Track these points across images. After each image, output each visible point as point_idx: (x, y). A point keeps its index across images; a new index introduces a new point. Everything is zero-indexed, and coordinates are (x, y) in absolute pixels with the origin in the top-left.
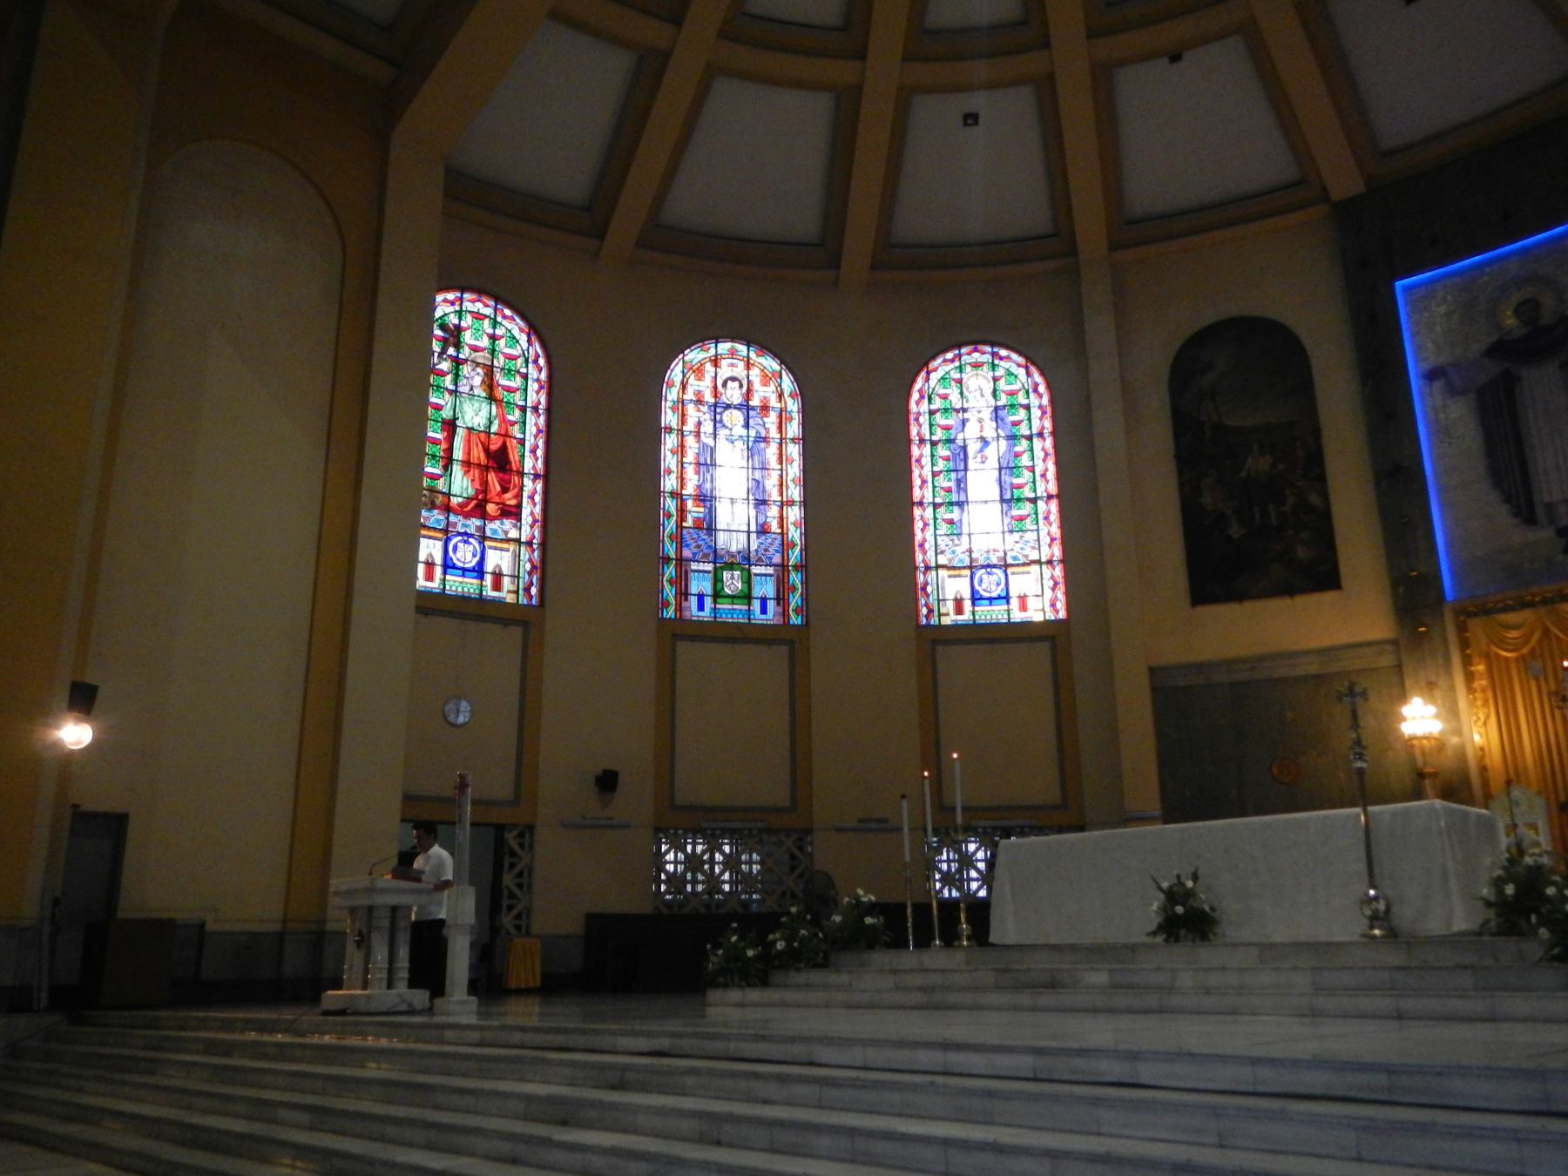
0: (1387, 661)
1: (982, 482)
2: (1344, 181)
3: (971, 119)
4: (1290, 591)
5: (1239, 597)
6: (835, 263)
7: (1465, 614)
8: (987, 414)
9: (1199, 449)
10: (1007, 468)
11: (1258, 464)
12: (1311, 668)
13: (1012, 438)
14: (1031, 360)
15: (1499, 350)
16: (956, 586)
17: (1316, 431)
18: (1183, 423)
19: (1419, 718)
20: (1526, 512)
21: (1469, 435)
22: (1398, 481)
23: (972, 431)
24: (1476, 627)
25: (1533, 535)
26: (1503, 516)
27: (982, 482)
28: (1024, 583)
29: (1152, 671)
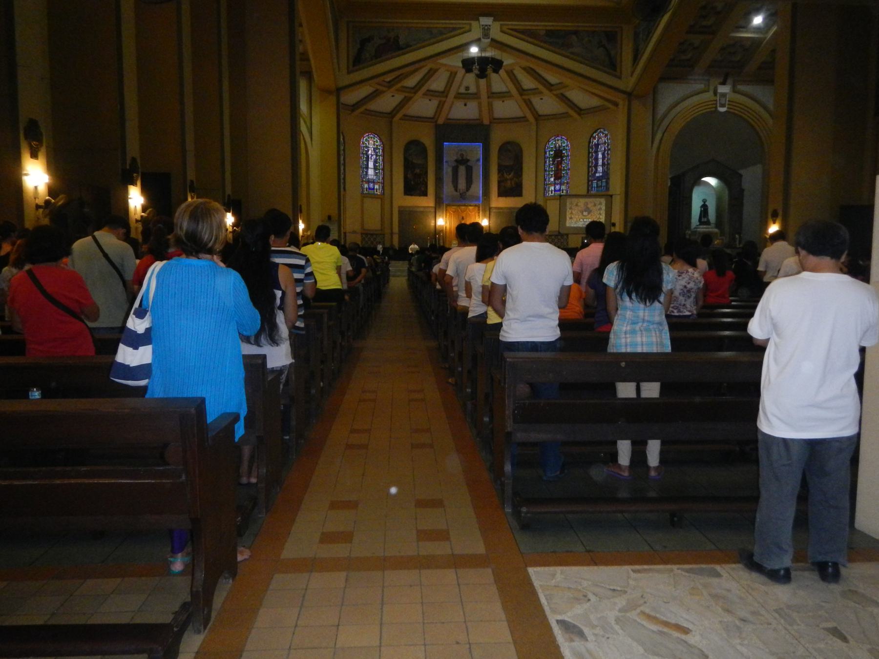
0: (433, 210)
1: (371, 164)
2: (441, 121)
4: (420, 195)
5: (411, 195)
6: (353, 111)
7: (447, 205)
9: (408, 166)
10: (375, 162)
11: (418, 171)
12: (422, 209)
13: (377, 155)
14: (380, 139)
15: (456, 161)
16: (366, 186)
17: (427, 168)
18: (406, 159)
19: (441, 222)
20: (456, 190)
21: (451, 173)
22: (439, 181)
24: (448, 208)
25: (455, 193)
26: (453, 189)
27: (371, 164)
28: (376, 187)
29: (399, 207)
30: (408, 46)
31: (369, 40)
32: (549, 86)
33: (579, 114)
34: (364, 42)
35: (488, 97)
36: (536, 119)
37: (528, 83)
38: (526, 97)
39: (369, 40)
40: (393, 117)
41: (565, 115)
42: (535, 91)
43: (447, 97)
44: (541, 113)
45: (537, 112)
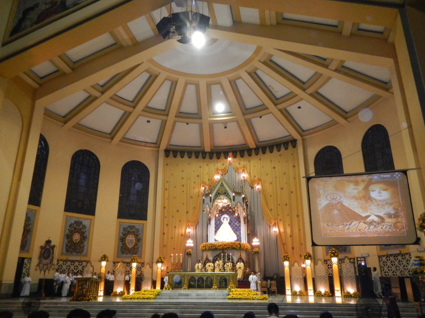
3: (148, 122)
6: (112, 139)
8: (136, 176)
23: (133, 179)
30: (75, 4)
31: (32, 9)
32: (301, 85)
33: (346, 119)
34: (26, 12)
35: (244, 114)
36: (301, 136)
37: (280, 87)
38: (280, 106)
39: (32, 9)
40: (159, 147)
41: (332, 124)
42: (291, 96)
43: (201, 118)
44: (305, 128)
45: (300, 127)
